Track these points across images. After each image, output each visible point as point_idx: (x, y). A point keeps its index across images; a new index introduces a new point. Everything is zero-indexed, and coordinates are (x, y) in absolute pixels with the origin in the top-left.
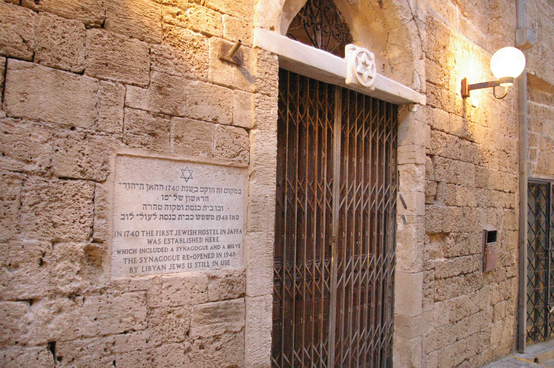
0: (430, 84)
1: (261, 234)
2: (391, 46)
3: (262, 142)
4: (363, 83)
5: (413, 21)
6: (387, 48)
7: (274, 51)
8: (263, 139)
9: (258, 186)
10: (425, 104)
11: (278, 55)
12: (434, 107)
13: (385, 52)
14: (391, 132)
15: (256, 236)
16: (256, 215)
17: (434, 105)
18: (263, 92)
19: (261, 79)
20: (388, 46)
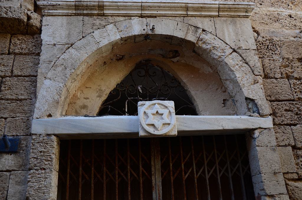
0: (280, 103)
4: (156, 133)
5: (234, 54)
6: (224, 85)
7: (49, 133)
10: (271, 126)
11: (55, 135)
12: (295, 125)
13: (223, 88)
17: (293, 122)
18: (36, 168)
20: (223, 83)
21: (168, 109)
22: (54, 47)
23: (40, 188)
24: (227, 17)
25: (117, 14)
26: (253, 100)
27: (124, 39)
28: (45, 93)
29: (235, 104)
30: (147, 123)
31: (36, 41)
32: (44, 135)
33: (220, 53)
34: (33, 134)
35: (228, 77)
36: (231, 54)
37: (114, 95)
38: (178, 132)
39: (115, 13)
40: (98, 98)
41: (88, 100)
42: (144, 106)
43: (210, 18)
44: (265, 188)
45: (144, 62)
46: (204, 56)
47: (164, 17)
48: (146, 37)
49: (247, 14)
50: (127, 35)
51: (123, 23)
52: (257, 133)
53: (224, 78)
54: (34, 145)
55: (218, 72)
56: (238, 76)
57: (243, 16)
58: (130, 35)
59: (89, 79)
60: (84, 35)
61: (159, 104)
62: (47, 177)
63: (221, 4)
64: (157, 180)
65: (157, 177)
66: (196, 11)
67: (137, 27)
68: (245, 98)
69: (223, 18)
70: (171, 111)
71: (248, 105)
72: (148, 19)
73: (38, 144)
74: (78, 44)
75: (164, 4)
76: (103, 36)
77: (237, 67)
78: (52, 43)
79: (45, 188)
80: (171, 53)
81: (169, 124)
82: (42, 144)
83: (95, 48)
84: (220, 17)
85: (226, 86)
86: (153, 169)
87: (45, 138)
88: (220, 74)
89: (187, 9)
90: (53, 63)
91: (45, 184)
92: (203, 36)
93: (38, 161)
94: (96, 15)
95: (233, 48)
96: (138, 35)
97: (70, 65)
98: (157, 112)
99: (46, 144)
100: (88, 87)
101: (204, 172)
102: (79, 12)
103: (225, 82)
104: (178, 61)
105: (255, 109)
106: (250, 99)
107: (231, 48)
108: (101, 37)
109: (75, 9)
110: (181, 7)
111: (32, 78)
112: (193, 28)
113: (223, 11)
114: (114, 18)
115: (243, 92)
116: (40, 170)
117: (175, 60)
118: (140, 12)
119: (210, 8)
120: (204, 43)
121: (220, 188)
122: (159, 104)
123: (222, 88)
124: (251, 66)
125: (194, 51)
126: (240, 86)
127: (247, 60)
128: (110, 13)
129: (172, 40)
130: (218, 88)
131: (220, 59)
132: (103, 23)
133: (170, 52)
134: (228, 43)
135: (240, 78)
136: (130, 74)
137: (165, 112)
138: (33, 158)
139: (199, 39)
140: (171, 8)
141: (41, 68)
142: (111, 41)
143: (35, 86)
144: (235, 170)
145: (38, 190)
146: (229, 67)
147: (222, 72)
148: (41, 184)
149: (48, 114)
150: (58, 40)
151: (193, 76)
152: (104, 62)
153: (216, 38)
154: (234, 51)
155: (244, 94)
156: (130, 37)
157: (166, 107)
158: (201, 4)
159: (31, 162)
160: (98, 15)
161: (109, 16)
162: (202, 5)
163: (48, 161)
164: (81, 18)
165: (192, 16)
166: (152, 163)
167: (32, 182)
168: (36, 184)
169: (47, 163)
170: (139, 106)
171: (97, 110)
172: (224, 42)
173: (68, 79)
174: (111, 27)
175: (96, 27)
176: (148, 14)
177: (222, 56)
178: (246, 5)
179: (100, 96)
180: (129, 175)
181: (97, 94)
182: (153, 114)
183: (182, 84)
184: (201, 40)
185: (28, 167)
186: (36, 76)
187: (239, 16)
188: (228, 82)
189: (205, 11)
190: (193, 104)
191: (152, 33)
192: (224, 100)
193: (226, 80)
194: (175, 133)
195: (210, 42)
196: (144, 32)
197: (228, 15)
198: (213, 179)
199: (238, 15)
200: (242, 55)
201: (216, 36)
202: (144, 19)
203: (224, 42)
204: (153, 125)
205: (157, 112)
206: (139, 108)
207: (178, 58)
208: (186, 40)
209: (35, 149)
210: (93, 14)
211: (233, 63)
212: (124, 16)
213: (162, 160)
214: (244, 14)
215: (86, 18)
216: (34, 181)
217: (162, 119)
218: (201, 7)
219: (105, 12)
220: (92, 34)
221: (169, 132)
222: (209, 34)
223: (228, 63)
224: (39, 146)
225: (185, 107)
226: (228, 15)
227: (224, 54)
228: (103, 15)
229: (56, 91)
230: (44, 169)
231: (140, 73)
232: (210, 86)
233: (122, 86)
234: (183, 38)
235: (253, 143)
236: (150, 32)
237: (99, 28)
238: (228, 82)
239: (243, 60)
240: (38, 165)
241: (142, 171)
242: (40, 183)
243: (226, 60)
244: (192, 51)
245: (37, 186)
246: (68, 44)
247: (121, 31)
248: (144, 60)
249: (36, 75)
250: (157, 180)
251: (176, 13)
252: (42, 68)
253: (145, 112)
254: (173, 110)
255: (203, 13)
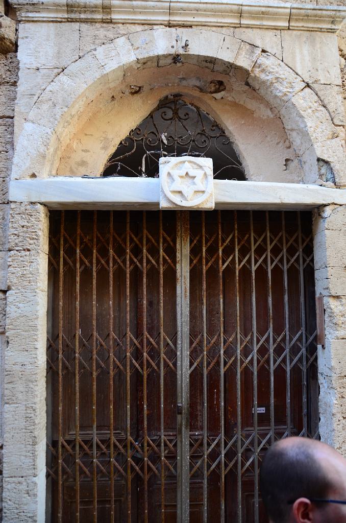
1: (17, 407)
2: (291, 133)
3: (16, 304)
5: (307, 90)
6: (288, 137)
7: (33, 200)
8: (17, 300)
9: (12, 354)
13: (287, 141)
14: (300, 252)
15: (11, 409)
16: (10, 386)
18: (17, 248)
19: (16, 235)
20: (288, 134)
21: (203, 170)
22: (37, 73)
23: (24, 275)
24: (301, 30)
25: (132, 20)
26: (327, 163)
27: (142, 61)
28: (25, 143)
29: (302, 166)
30: (171, 189)
31: (10, 62)
32: (26, 203)
33: (286, 88)
34: (11, 202)
35: (294, 126)
36: (302, 90)
37: (126, 146)
38: (216, 204)
39: (129, 19)
40: (103, 151)
41: (88, 153)
42: (167, 164)
43: (275, 31)
44: (330, 286)
45: (172, 97)
46: (262, 92)
47: (203, 27)
48: (176, 58)
49: (333, 27)
50: (146, 56)
51: (141, 35)
52: (328, 211)
53: (289, 127)
54: (13, 217)
55: (281, 117)
56: (309, 124)
57: (327, 29)
58: (151, 54)
59: (90, 121)
60: (81, 54)
61: (190, 162)
62: (32, 261)
63: (294, 8)
64: (183, 270)
65: (183, 265)
66: (254, 18)
67: (162, 43)
68: (316, 159)
69: (295, 32)
70: (207, 173)
71: (320, 169)
72: (180, 30)
73: (19, 215)
74: (73, 68)
75: (205, 5)
76: (110, 56)
77: (310, 111)
78: (34, 66)
79: (31, 275)
80: (213, 85)
81: (203, 192)
82: (24, 216)
83: (98, 75)
84: (291, 30)
85: (291, 140)
86: (178, 255)
87: (28, 207)
88: (284, 121)
89: (240, 14)
90: (36, 98)
91: (31, 270)
92: (263, 60)
93: (20, 240)
94: (99, 22)
95: (306, 81)
96: (164, 55)
97: (60, 102)
98: (187, 174)
99: (29, 216)
100: (88, 134)
101: (249, 261)
102: (73, 16)
103: (291, 133)
104: (222, 98)
105: (329, 176)
106: (323, 161)
107: (303, 81)
108: (107, 57)
109: (68, 12)
110: (232, 11)
111: (7, 119)
112: (248, 46)
113: (297, 20)
114: (128, 28)
115: (314, 149)
116: (23, 251)
117: (218, 96)
118: (167, 18)
119: (276, 14)
120: (263, 71)
121: (270, 283)
122: (190, 162)
123: (285, 142)
124: (331, 111)
125: (247, 84)
126: (310, 140)
127: (326, 102)
128: (121, 19)
129: (214, 64)
130: (278, 141)
131: (285, 98)
132: (111, 35)
133: (211, 82)
134: (299, 73)
135: (312, 129)
136: (151, 116)
137: (199, 173)
138: (13, 234)
139: (256, 65)
140: (215, 13)
141: (19, 105)
142: (121, 64)
143: (12, 133)
144: (293, 260)
145: (22, 278)
146: (298, 111)
147: (287, 117)
148: (25, 270)
149: (31, 173)
150: (43, 62)
151: (243, 123)
152: (111, 96)
153: (282, 64)
154: (308, 86)
155: (315, 153)
156: (150, 59)
157: (201, 167)
158: (263, 7)
159: (10, 241)
160: (103, 21)
161: (119, 23)
162: (263, 9)
163: (33, 239)
164: (76, 26)
165: (248, 27)
166: (178, 246)
167: (13, 267)
168: (19, 269)
169: (32, 242)
170: (161, 164)
171: (101, 169)
172: (293, 71)
173: (59, 122)
174: (121, 41)
175: (100, 41)
176: (179, 21)
177: (287, 93)
178: (333, 10)
179: (105, 148)
180: (145, 261)
181: (101, 145)
182: (181, 177)
183: (227, 134)
184: (259, 67)
185: (7, 246)
186: (12, 118)
187: (321, 30)
188: (294, 134)
189: (268, 19)
190: (241, 164)
191: (184, 53)
192: (287, 160)
193: (292, 130)
194: (211, 205)
195: (271, 70)
196: (173, 51)
197: (303, 27)
198: (261, 271)
199: (318, 28)
200: (319, 93)
201: (282, 61)
202: (173, 29)
203: (293, 71)
204: (180, 192)
205: (187, 174)
206: (160, 166)
207: (223, 93)
208: (236, 66)
209: (15, 223)
210: (94, 19)
211: (305, 105)
212: (143, 24)
213: (191, 242)
214: (329, 26)
215: (84, 27)
216: (16, 266)
217: (194, 184)
218: (263, 13)
219: (115, 16)
220: (94, 52)
221: (202, 203)
222: (272, 58)
223: (297, 105)
224: (20, 218)
225: (229, 168)
226: (303, 27)
227: (291, 90)
228: (111, 22)
229: (41, 139)
230: (29, 250)
231: (165, 115)
232: (268, 139)
233: (137, 134)
234: (231, 61)
235: (322, 225)
236: (181, 51)
237: (104, 44)
238: (294, 134)
239: (320, 101)
240: (20, 244)
241: (163, 256)
242: (24, 268)
243: (293, 100)
244: (244, 83)
245: (21, 273)
246: (57, 68)
247: (138, 48)
248: (171, 95)
249: (12, 116)
250: (183, 270)
251: (223, 21)
252: (21, 106)
253: (169, 174)
254: (210, 172)
255: (266, 23)
